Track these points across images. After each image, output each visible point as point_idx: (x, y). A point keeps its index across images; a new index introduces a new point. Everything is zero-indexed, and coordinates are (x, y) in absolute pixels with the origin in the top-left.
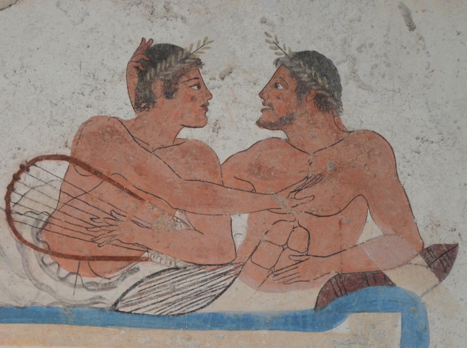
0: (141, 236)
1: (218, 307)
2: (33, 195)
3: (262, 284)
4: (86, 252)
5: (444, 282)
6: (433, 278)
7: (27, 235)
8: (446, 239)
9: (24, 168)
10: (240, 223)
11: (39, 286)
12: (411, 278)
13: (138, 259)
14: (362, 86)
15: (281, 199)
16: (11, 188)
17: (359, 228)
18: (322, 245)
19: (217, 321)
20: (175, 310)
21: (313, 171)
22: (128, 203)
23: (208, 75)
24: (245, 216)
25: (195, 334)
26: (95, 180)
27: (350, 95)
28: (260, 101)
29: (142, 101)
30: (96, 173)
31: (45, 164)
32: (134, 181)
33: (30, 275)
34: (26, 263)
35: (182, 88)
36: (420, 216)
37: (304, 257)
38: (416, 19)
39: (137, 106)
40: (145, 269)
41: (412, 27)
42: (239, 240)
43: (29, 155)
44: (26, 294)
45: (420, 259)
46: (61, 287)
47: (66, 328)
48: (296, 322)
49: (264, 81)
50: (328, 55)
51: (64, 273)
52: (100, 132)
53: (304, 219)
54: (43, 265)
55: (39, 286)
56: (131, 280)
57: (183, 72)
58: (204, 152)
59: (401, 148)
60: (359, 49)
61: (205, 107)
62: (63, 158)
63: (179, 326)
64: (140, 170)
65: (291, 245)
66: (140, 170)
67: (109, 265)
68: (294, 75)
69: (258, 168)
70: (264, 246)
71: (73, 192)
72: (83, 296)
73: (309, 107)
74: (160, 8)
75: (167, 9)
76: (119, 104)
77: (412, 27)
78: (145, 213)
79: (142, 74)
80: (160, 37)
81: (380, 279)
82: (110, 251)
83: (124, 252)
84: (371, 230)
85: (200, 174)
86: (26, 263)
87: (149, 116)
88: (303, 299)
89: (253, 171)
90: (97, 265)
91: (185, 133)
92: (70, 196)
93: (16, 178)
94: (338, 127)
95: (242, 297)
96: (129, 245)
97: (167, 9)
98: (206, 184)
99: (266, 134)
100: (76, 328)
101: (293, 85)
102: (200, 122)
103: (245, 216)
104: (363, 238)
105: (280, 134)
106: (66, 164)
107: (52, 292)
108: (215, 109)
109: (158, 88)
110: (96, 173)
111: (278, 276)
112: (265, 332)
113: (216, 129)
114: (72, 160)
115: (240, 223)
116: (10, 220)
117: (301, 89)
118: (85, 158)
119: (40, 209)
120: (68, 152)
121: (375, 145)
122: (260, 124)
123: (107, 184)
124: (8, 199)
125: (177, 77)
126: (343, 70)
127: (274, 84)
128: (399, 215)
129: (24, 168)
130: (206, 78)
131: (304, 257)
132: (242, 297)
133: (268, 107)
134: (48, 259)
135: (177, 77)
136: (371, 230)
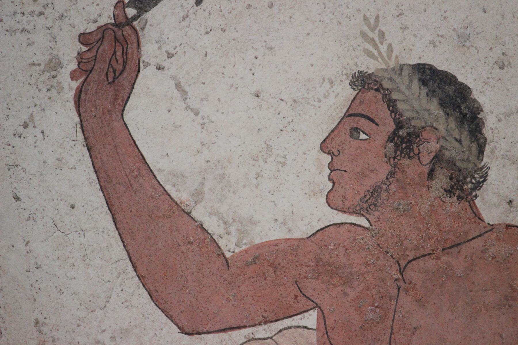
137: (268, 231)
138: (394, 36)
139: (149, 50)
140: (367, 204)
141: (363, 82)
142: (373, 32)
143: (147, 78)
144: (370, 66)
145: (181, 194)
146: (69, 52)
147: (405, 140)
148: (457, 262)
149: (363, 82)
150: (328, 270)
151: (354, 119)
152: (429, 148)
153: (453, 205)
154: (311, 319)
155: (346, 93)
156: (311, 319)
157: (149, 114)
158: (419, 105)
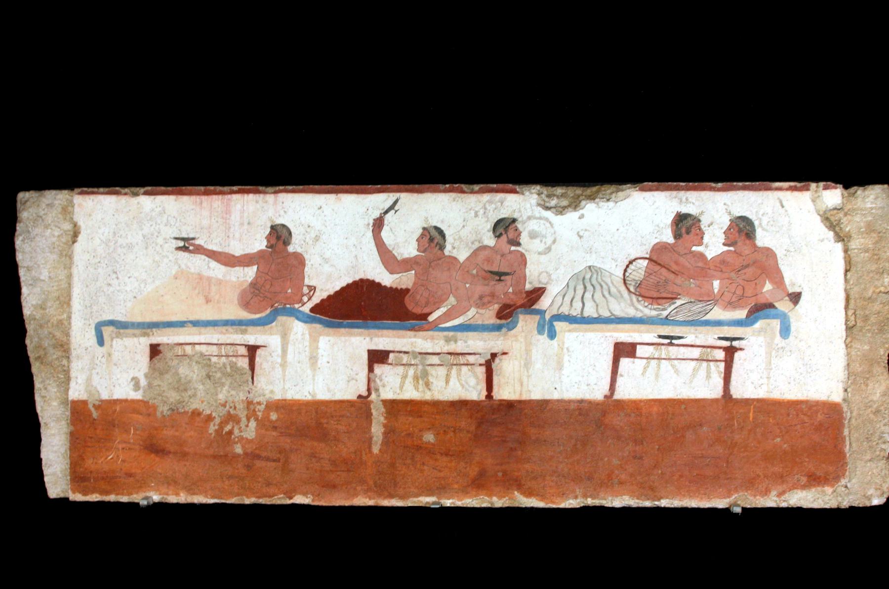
0: (677, 289)
1: (708, 317)
2: (634, 273)
3: (725, 308)
4: (655, 296)
5: (798, 306)
6: (792, 306)
7: (632, 289)
8: (797, 290)
9: (631, 262)
10: (716, 284)
11: (637, 309)
12: (783, 306)
13: (676, 298)
14: (763, 229)
15: (733, 275)
16: (625, 271)
17: (763, 286)
18: (749, 292)
19: (707, 323)
20: (690, 319)
21: (745, 263)
22: (672, 276)
23: (704, 225)
24: (718, 281)
25: (699, 328)
26: (659, 267)
27: (759, 233)
28: (723, 236)
29: (677, 236)
30: (659, 264)
31: (639, 261)
32: (674, 267)
33: (633, 305)
34: (631, 300)
35: (693, 230)
36: (787, 281)
37: (742, 297)
38: (784, 203)
39: (675, 238)
40: (679, 302)
41: (783, 207)
42: (716, 291)
43: (633, 257)
44: (631, 312)
45: (787, 298)
46: (646, 310)
47: (647, 326)
48: (739, 323)
49: (725, 228)
50: (750, 217)
51: (646, 304)
52: (660, 249)
53: (741, 282)
54: (638, 301)
55: (637, 309)
56: (673, 307)
57: (693, 224)
58: (702, 256)
59: (780, 253)
60: (763, 215)
61: (702, 238)
62: (646, 258)
63: (692, 325)
64: (677, 263)
65: (737, 292)
66: (677, 263)
67: (664, 301)
68: (737, 225)
69: (723, 262)
70: (726, 293)
71: (650, 272)
72: (654, 313)
73: (743, 238)
74: (684, 199)
75: (687, 199)
76: (668, 237)
77: (783, 207)
78: (679, 280)
79: (677, 225)
80: (684, 210)
81: (771, 306)
82: (664, 295)
83: (670, 296)
84: (768, 286)
85: (700, 264)
86: (631, 300)
87: (680, 241)
88: (741, 314)
89: (721, 262)
90: (660, 301)
91: (694, 248)
92: (648, 273)
93: (627, 266)
94: (755, 245)
95: (717, 313)
96: (672, 293)
97: (687, 199)
98: (703, 269)
99: (726, 248)
100: (651, 326)
101: (737, 229)
102: (700, 244)
103: (718, 281)
104: (765, 290)
105: (732, 249)
106: (647, 261)
107: (642, 311)
108: (706, 239)
109: (683, 230)
110: (659, 264)
111: (731, 305)
112: (726, 328)
113: (707, 246)
114: (650, 259)
115: (716, 284)
116: (625, 283)
117: (740, 231)
118: (654, 258)
119: (637, 279)
120: (648, 256)
121: (769, 253)
122: (724, 244)
123: (663, 269)
124: (624, 275)
125: (691, 226)
126: (756, 223)
127: (729, 229)
128: (778, 280)
129: (631, 262)
130: (702, 227)
131: (742, 297)
132: (717, 313)
133: (727, 238)
134: (640, 299)
135: (691, 226)
136: (768, 286)
137: (406, 256)
138: (430, 221)
139: (386, 222)
140: (423, 252)
141: (424, 229)
142: (426, 220)
143: (385, 227)
144: (426, 226)
145: (391, 249)
146: (371, 222)
147: (431, 239)
148: (440, 262)
149: (424, 229)
150: (417, 263)
151: (422, 236)
152: (436, 241)
153: (440, 252)
154: (413, 272)
155: (421, 231)
156: (413, 272)
157: (385, 234)
158: (434, 233)
